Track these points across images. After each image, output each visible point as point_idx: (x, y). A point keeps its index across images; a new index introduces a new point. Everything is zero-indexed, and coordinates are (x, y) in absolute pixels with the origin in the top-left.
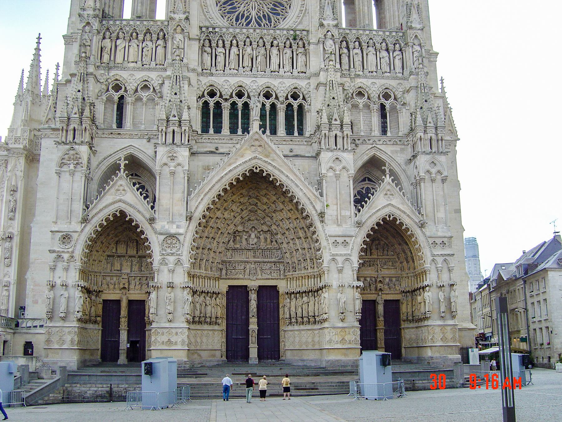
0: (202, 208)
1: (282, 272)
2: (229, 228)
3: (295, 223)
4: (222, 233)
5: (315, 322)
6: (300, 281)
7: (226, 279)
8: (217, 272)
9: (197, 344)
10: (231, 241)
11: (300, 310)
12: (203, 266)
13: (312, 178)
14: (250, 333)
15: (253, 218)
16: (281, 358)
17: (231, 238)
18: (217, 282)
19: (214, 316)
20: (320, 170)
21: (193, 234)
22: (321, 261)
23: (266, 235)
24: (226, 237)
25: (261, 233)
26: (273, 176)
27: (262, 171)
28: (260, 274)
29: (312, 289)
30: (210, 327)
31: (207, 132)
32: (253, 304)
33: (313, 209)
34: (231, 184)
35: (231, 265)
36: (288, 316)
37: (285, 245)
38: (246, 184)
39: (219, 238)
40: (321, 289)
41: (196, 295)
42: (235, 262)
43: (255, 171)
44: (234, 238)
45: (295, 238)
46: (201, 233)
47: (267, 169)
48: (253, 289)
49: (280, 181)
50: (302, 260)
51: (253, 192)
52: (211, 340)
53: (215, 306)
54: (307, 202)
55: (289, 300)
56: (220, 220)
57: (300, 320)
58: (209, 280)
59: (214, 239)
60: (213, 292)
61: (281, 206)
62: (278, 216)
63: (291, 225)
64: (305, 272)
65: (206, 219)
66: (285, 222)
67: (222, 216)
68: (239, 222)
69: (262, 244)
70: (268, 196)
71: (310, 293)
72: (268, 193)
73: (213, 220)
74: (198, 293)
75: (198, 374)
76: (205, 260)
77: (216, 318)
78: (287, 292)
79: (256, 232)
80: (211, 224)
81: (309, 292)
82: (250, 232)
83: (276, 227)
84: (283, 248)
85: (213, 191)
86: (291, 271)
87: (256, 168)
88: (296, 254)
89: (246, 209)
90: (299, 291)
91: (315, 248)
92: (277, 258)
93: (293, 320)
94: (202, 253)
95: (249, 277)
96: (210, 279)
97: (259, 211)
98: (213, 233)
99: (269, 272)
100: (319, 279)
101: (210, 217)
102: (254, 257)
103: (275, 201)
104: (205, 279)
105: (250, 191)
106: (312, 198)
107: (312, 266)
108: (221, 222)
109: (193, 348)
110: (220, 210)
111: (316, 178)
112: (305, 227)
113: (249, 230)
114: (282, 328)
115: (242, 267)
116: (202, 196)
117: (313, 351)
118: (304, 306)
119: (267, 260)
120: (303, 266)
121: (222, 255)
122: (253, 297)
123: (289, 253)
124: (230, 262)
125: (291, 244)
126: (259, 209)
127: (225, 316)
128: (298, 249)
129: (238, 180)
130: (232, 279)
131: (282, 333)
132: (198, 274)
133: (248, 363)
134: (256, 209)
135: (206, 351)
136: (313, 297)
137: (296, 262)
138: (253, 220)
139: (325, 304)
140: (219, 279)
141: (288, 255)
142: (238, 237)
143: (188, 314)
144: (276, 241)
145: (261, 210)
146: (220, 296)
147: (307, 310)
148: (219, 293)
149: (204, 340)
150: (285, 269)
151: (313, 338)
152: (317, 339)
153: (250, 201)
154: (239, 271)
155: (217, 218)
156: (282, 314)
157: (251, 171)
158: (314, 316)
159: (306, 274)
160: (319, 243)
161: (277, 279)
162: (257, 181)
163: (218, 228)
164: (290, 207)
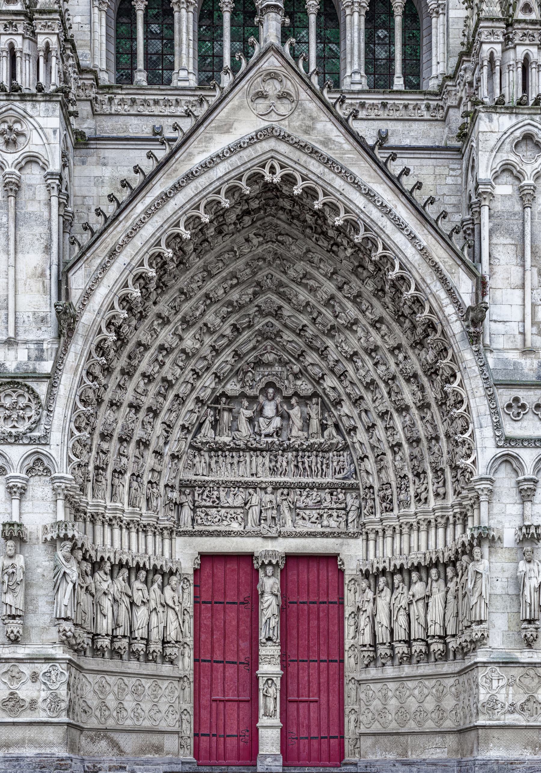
2: (199, 384)
3: (392, 361)
4: (177, 396)
15: (270, 357)
17: (206, 415)
24: (192, 411)
25: (293, 401)
27: (289, 180)
28: (289, 523)
31: (130, 79)
39: (170, 410)
43: (268, 178)
48: (270, 563)
63: (382, 368)
68: (229, 367)
69: (294, 433)
80: (143, 367)
82: (261, 399)
83: (335, 382)
97: (288, 336)
98: (151, 394)
99: (315, 514)
108: (175, 363)
112: (420, 372)
113: (257, 393)
138: (270, 365)
142: (226, 414)
145: (294, 331)
163: (164, 380)
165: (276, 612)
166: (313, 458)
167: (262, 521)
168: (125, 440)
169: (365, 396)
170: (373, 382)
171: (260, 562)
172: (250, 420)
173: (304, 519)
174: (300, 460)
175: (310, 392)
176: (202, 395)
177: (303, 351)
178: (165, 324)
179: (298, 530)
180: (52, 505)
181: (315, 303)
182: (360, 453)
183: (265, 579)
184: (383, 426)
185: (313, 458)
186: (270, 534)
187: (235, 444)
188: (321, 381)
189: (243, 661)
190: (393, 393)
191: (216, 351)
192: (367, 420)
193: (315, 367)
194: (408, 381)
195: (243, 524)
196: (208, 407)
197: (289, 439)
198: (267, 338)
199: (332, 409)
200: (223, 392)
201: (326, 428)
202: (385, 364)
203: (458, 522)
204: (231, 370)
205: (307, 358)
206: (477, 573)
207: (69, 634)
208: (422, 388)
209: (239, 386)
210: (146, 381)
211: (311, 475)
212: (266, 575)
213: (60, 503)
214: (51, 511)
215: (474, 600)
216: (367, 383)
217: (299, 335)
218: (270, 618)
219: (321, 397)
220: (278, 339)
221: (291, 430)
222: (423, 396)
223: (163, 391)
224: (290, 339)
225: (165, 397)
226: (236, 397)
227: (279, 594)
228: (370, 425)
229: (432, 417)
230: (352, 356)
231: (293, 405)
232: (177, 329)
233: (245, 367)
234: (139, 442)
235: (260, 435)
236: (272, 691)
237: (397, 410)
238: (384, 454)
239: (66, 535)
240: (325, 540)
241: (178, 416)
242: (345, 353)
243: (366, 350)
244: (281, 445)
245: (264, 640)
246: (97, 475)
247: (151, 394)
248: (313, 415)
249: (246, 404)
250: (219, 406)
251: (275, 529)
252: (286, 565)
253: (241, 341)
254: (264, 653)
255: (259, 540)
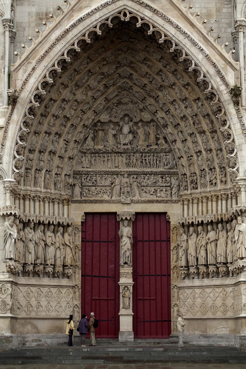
0: (34, 82)
1: (174, 190)
2: (85, 117)
4: (72, 125)
5: (227, 274)
6: (205, 204)
7: (80, 202)
8: (65, 191)
9: (31, 309)
10: (89, 139)
11: (203, 253)
12: (41, 181)
13: (223, 30)
14: (121, 291)
15: (126, 100)
16: (172, 333)
18: (66, 207)
19: (59, 263)
20: (235, 17)
21: (18, 127)
22: (234, 169)
23: (147, 128)
24: (81, 132)
25: (140, 124)
26: (154, 27)
28: (137, 195)
29: (222, 219)
30: (55, 282)
32: (126, 244)
33: (221, 83)
34: (82, 43)
35: (89, 178)
36: (183, 263)
37: (179, 145)
38: (112, 42)
39: (68, 133)
40: (234, 217)
41: (28, 228)
42: (96, 173)
44: (94, 134)
45: (196, 132)
46: (37, 126)
47: (142, 16)
48: (126, 219)
49: (165, 36)
50: (207, 170)
51: (123, 56)
52: (55, 303)
53: (62, 247)
54: (212, 71)
55: (185, 237)
56: (69, 104)
57: (202, 269)
58: (51, 204)
59: (60, 136)
60: (59, 223)
61: (172, 79)
62: (165, 96)
63: (189, 110)
64: (212, 189)
65: (45, 102)
66: (179, 105)
67: (70, 97)
68: (102, 106)
69: (140, 143)
70: (148, 63)
71: (220, 226)
72: (149, 57)
73: (56, 104)
74: (32, 225)
75: (27, 358)
76: (44, 170)
77: (64, 266)
78: (183, 223)
79: (131, 124)
80: (54, 109)
81: (217, 223)
82: (121, 124)
83: (164, 115)
84: (177, 150)
85: (52, 54)
86: (189, 188)
87: (125, 15)
88: (198, 160)
89: (113, 85)
90: (202, 221)
91: (227, 148)
92: (167, 167)
93: (192, 270)
94: (40, 160)
95: (118, 198)
96: (53, 202)
98: (57, 125)
100: (234, 201)
101: (51, 99)
102: (128, 165)
103: (161, 71)
104: (44, 201)
105: (120, 54)
106: (221, 64)
107: (224, 179)
108: (71, 107)
109: (23, 315)
110: (68, 86)
111: (229, 30)
112: (210, 113)
113: (119, 121)
114: (175, 284)
115: (108, 183)
116: (34, 62)
117: (224, 323)
118: (209, 246)
119: (149, 170)
120: (208, 179)
121: (74, 163)
122: (126, 231)
123: (185, 158)
124: (87, 173)
125: (189, 143)
126: (135, 84)
127: (79, 263)
128: (200, 152)
129: (93, 34)
130: (91, 202)
131: (174, 292)
132: (33, 194)
133: (118, 340)
134: (131, 84)
135: (46, 321)
136: (224, 232)
137: (197, 173)
138: (126, 104)
139: (240, 242)
140: (68, 201)
141: (184, 161)
142: (100, 132)
143: (11, 259)
144: (165, 138)
145: (139, 87)
146: (70, 229)
147: (214, 254)
148: (68, 225)
149: (44, 303)
150: (179, 185)
151: (224, 300)
152: (229, 302)
153: (120, 71)
154: (103, 188)
155: (64, 100)
156: (175, 259)
157: (115, 19)
158: (225, 264)
159: (213, 193)
160: (231, 139)
161: (167, 202)
162: (131, 38)
163: (65, 117)
164: (187, 79)
165: (130, 248)
166: (151, 157)
167: (122, 194)
168: (43, 152)
169: (180, 123)
170: (184, 116)
171: (120, 218)
172: (114, 136)
173: (146, 192)
174: (143, 158)
175: (149, 120)
176: (87, 123)
177: (145, 97)
178: (66, 88)
179: (143, 199)
180: (3, 196)
181: (151, 73)
182: (179, 155)
183: (123, 228)
184: (191, 141)
185: (151, 157)
186: (126, 202)
187: (105, 149)
188: (156, 114)
189: (111, 276)
190: (196, 124)
191: (95, 99)
192: (182, 137)
193: (152, 106)
194: (204, 117)
195: (110, 196)
196: (90, 129)
197: (137, 146)
198: (124, 90)
199: (162, 129)
200: (99, 120)
201: (159, 139)
202: (191, 108)
203: (233, 198)
204: (104, 108)
205: (147, 101)
206: (240, 231)
207: (12, 267)
208: (212, 122)
209: (107, 117)
210: (55, 118)
211: (150, 167)
212: (124, 226)
213: (8, 195)
214: (3, 199)
215: (239, 246)
216: (181, 117)
217: (142, 89)
218: (126, 251)
219: (156, 122)
220: (131, 91)
221: (138, 141)
222: (212, 126)
223: (64, 123)
224: (137, 91)
225: (65, 126)
226: (106, 122)
227: (131, 237)
228: (184, 140)
229: (218, 138)
230: (172, 102)
231: (139, 127)
232: (72, 90)
233: (111, 106)
234: (50, 152)
235: (121, 144)
236: (127, 294)
237: (199, 133)
238: (192, 156)
239: (11, 213)
240: (159, 204)
241: (72, 136)
242: (169, 100)
243: (180, 100)
244: (133, 150)
245: (123, 264)
246: (27, 173)
247: (57, 125)
248: (151, 132)
249: (112, 126)
250: (96, 129)
251: (129, 199)
252: (136, 219)
253: (109, 92)
254: (122, 272)
255: (120, 205)
